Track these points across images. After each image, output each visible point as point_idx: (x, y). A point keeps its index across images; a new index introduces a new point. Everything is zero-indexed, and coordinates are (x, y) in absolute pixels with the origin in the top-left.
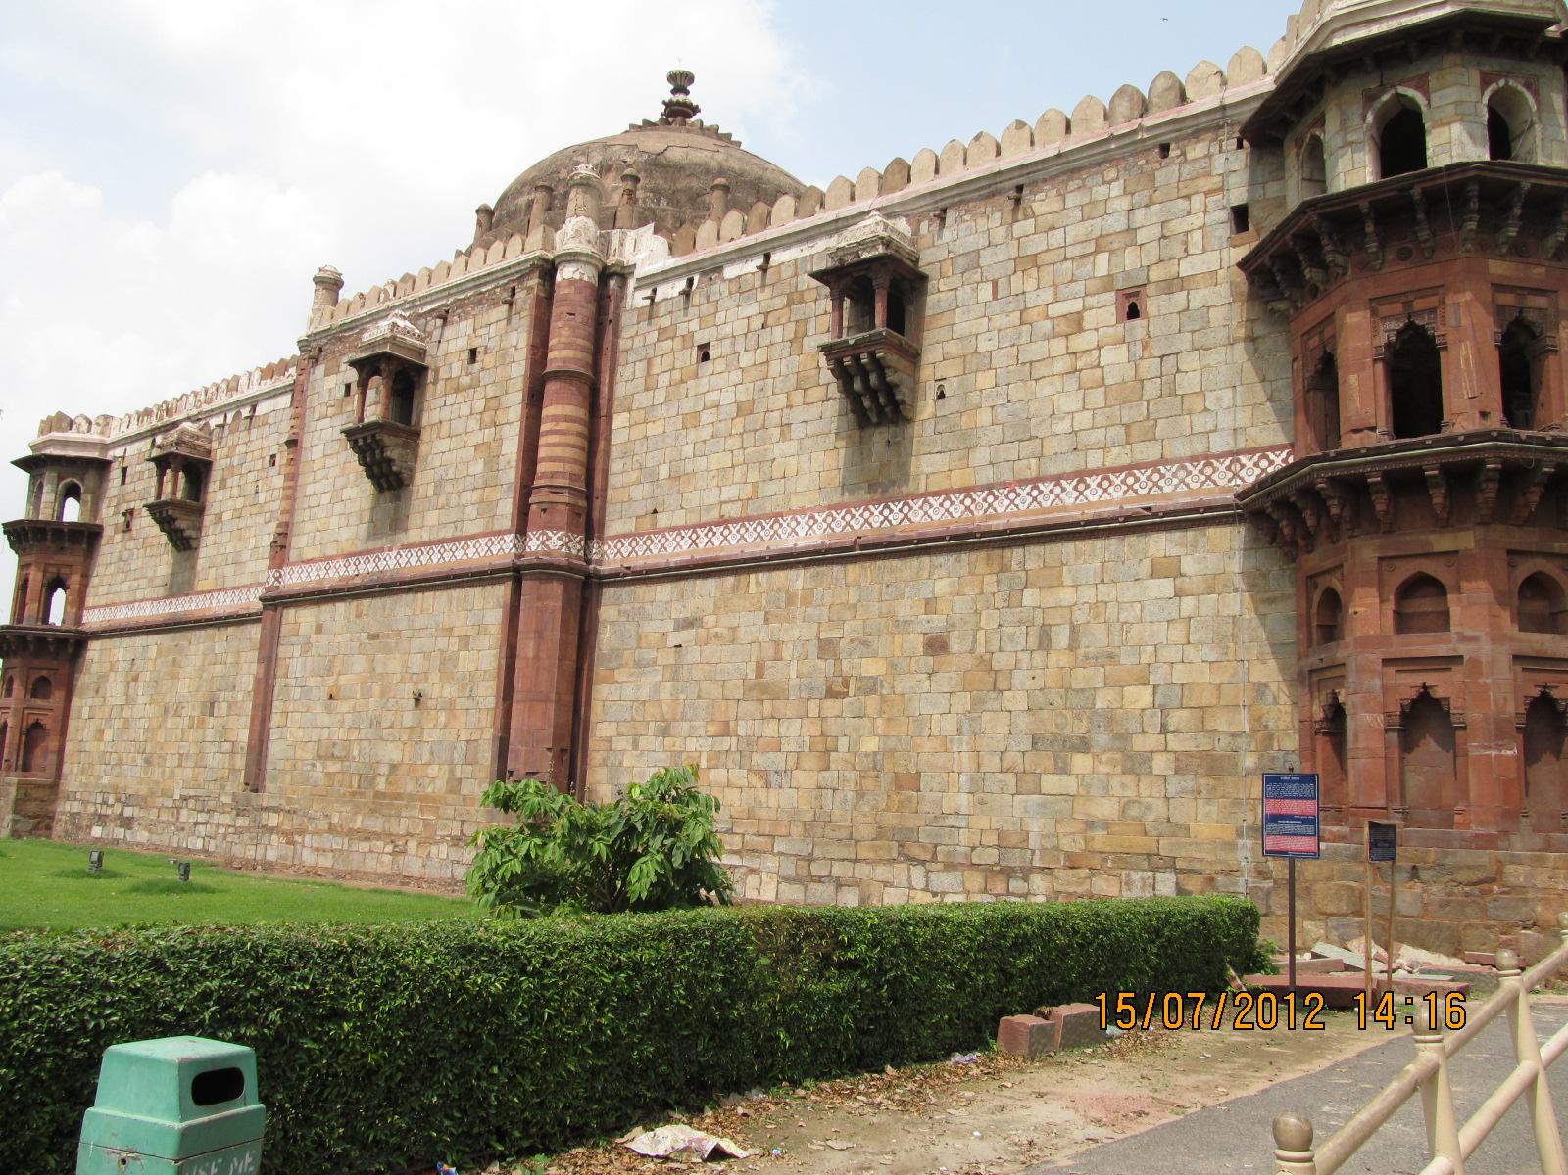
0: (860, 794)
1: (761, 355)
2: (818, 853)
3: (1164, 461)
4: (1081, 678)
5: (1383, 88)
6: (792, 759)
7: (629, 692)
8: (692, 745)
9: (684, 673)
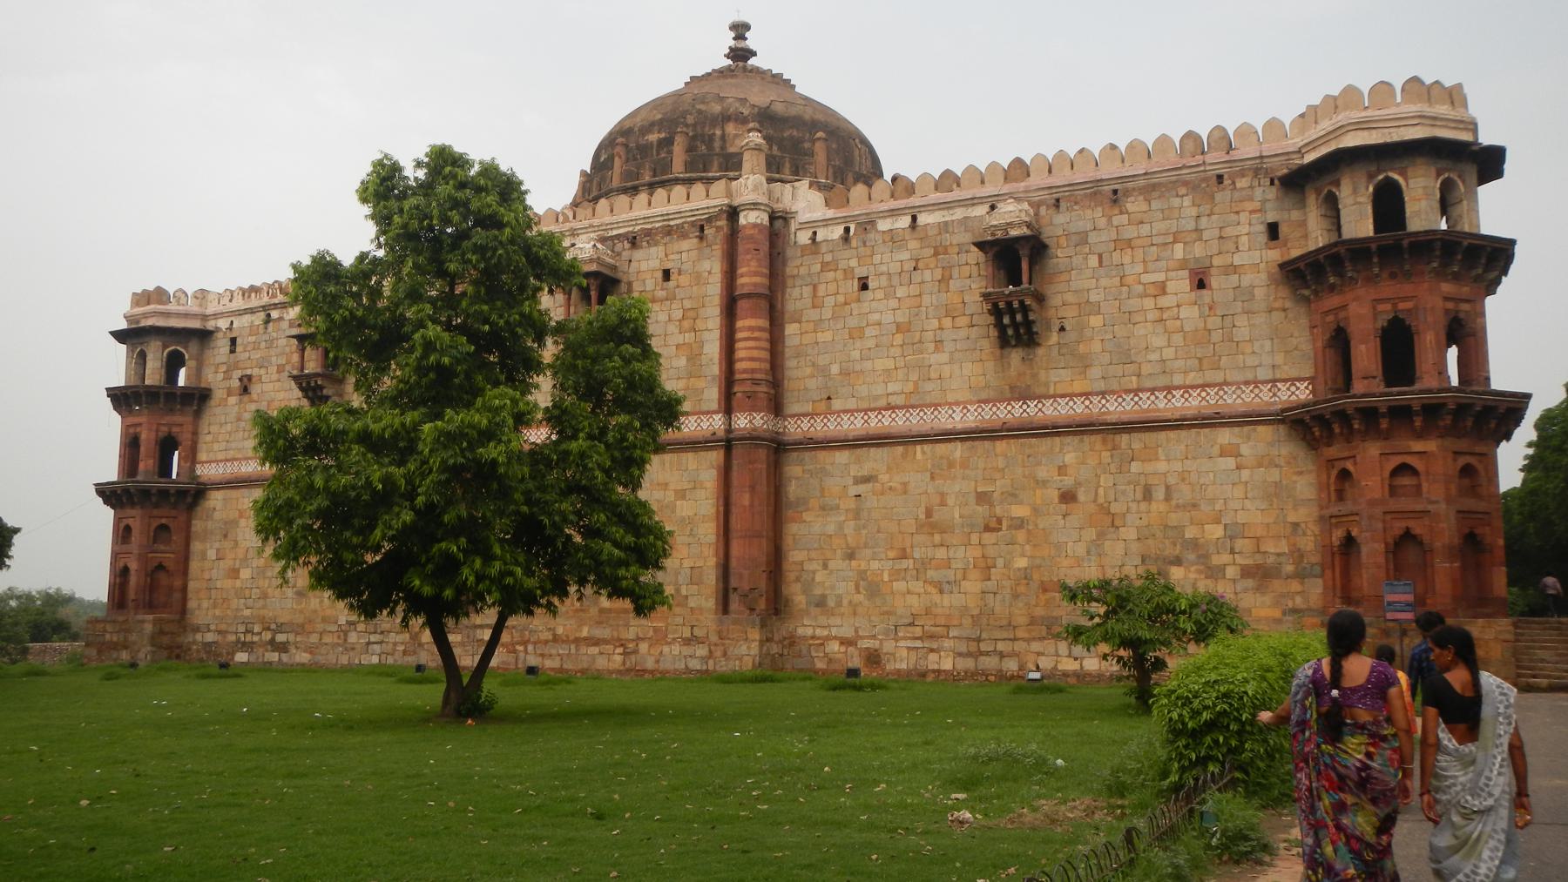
0: (1016, 596)
1: (914, 290)
2: (984, 636)
3: (1226, 383)
4: (1174, 518)
5: (1379, 172)
6: (959, 576)
7: (817, 528)
8: (875, 565)
9: (865, 514)
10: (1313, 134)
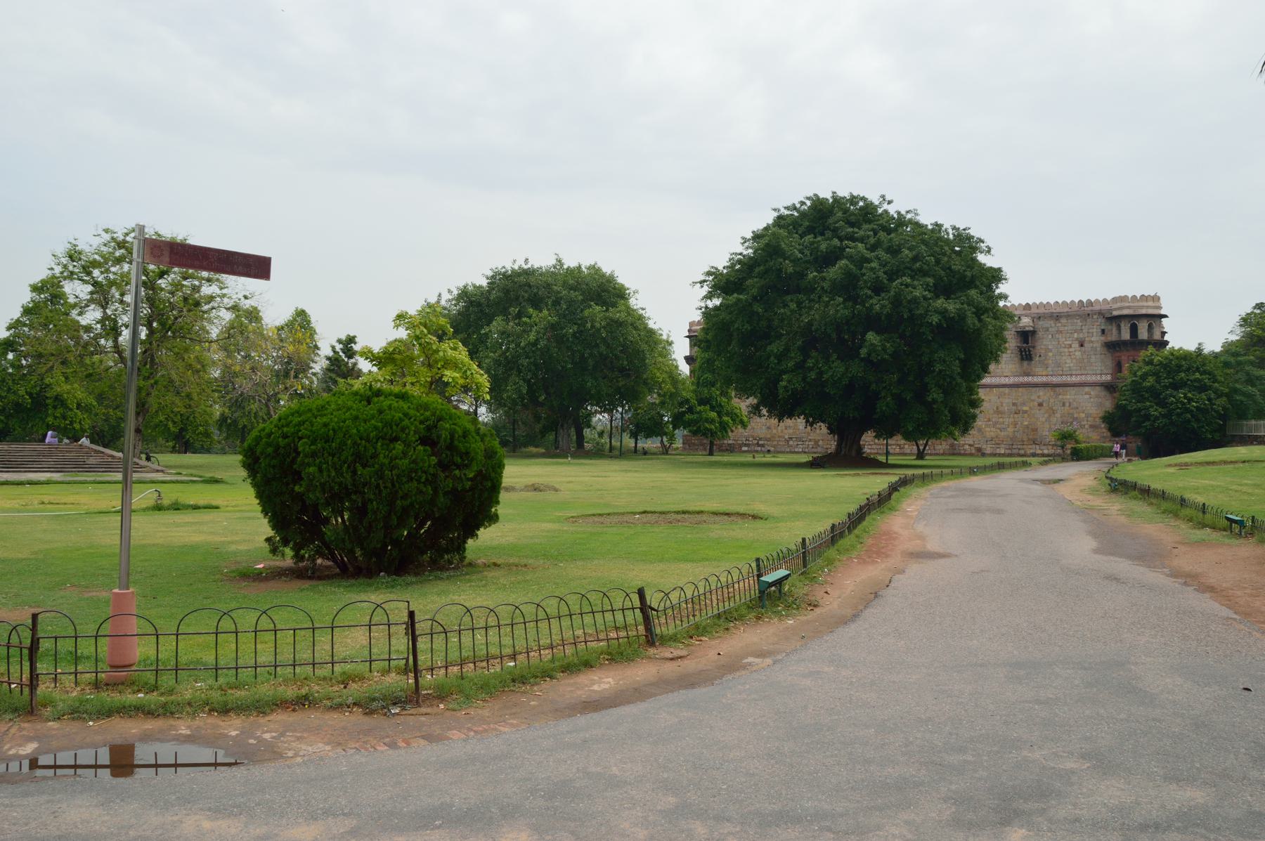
10: (1115, 306)
